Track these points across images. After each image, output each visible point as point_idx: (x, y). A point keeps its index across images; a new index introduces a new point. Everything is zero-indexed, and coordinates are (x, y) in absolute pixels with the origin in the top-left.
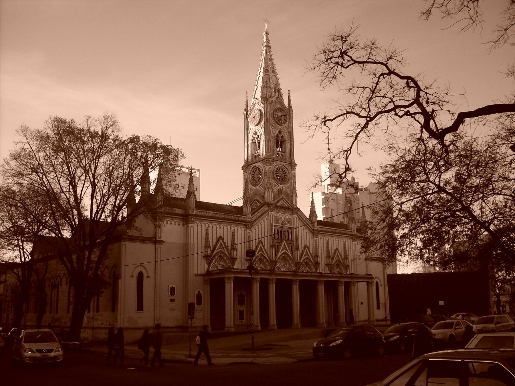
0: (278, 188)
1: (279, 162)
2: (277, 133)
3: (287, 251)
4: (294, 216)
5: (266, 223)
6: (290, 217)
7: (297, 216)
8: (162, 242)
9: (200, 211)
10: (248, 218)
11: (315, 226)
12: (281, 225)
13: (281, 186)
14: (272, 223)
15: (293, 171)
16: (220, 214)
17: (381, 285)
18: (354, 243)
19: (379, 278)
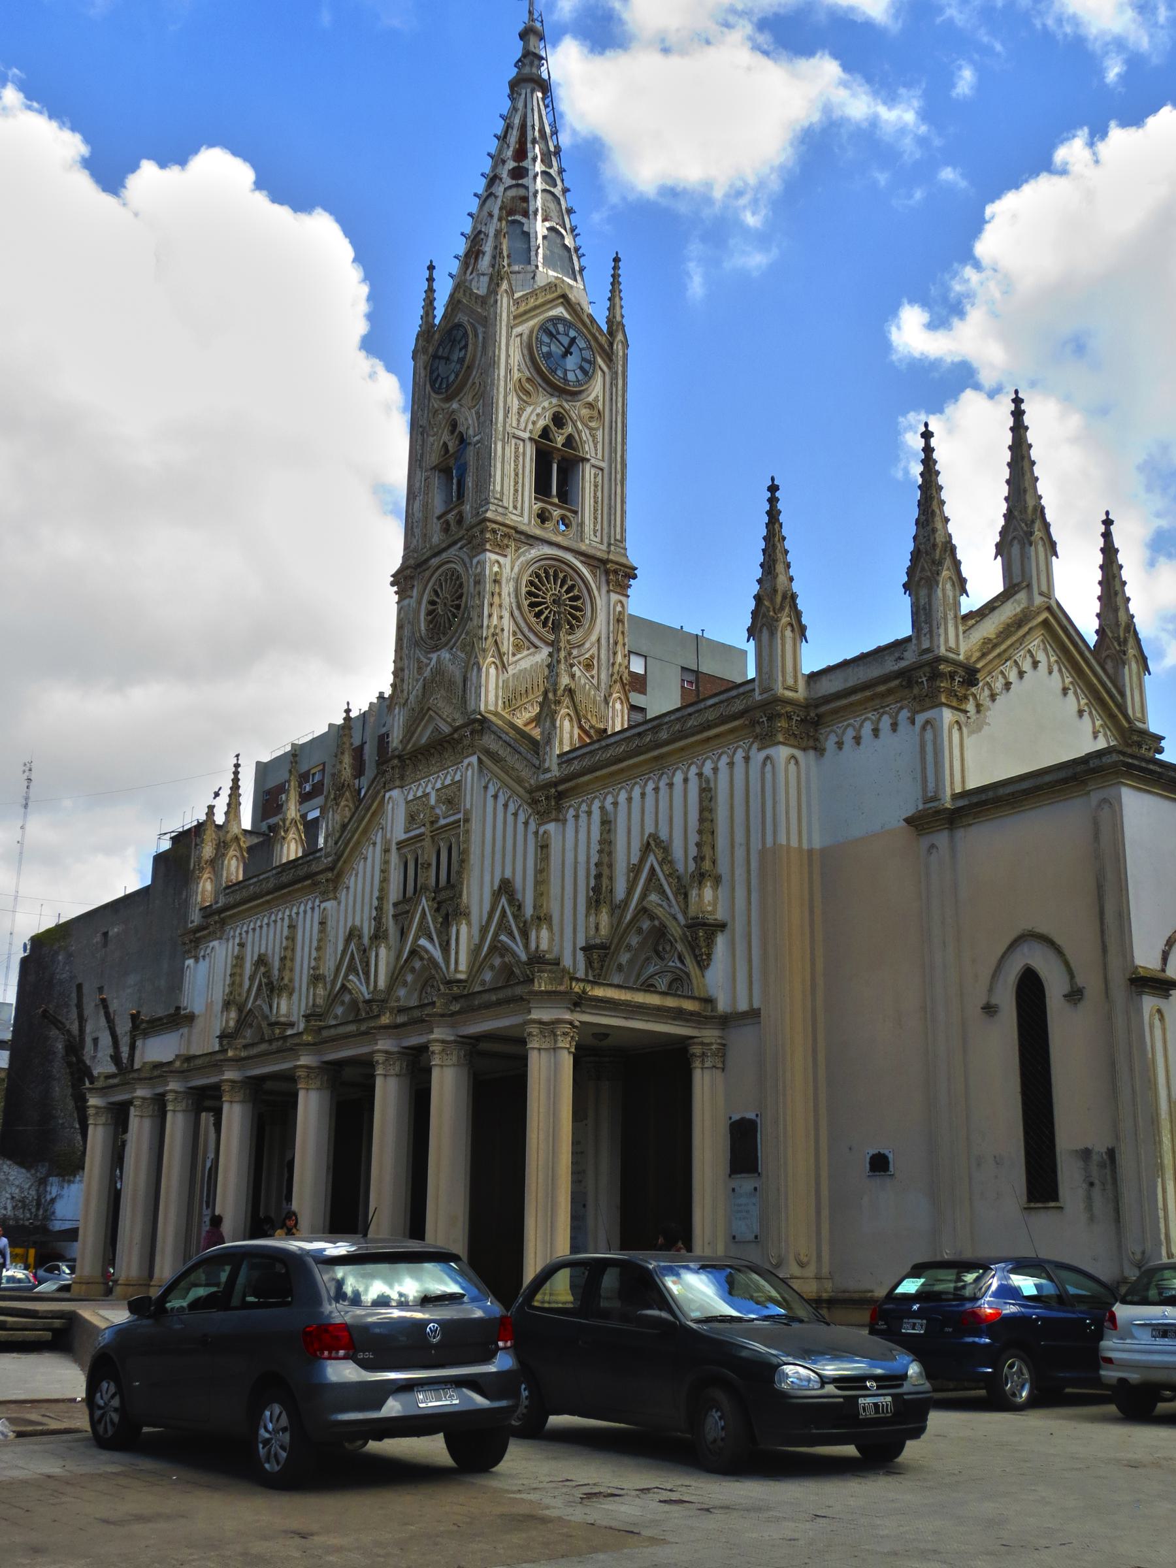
0: (427, 673)
1: (435, 562)
2: (446, 437)
3: (431, 939)
4: (466, 762)
5: (378, 847)
6: (457, 778)
7: (474, 759)
8: (191, 1018)
9: (232, 892)
10: (326, 856)
11: (547, 765)
12: (422, 830)
13: (434, 656)
14: (388, 836)
15: (475, 561)
16: (268, 878)
17: (1075, 995)
18: (762, 755)
19: (1059, 941)
